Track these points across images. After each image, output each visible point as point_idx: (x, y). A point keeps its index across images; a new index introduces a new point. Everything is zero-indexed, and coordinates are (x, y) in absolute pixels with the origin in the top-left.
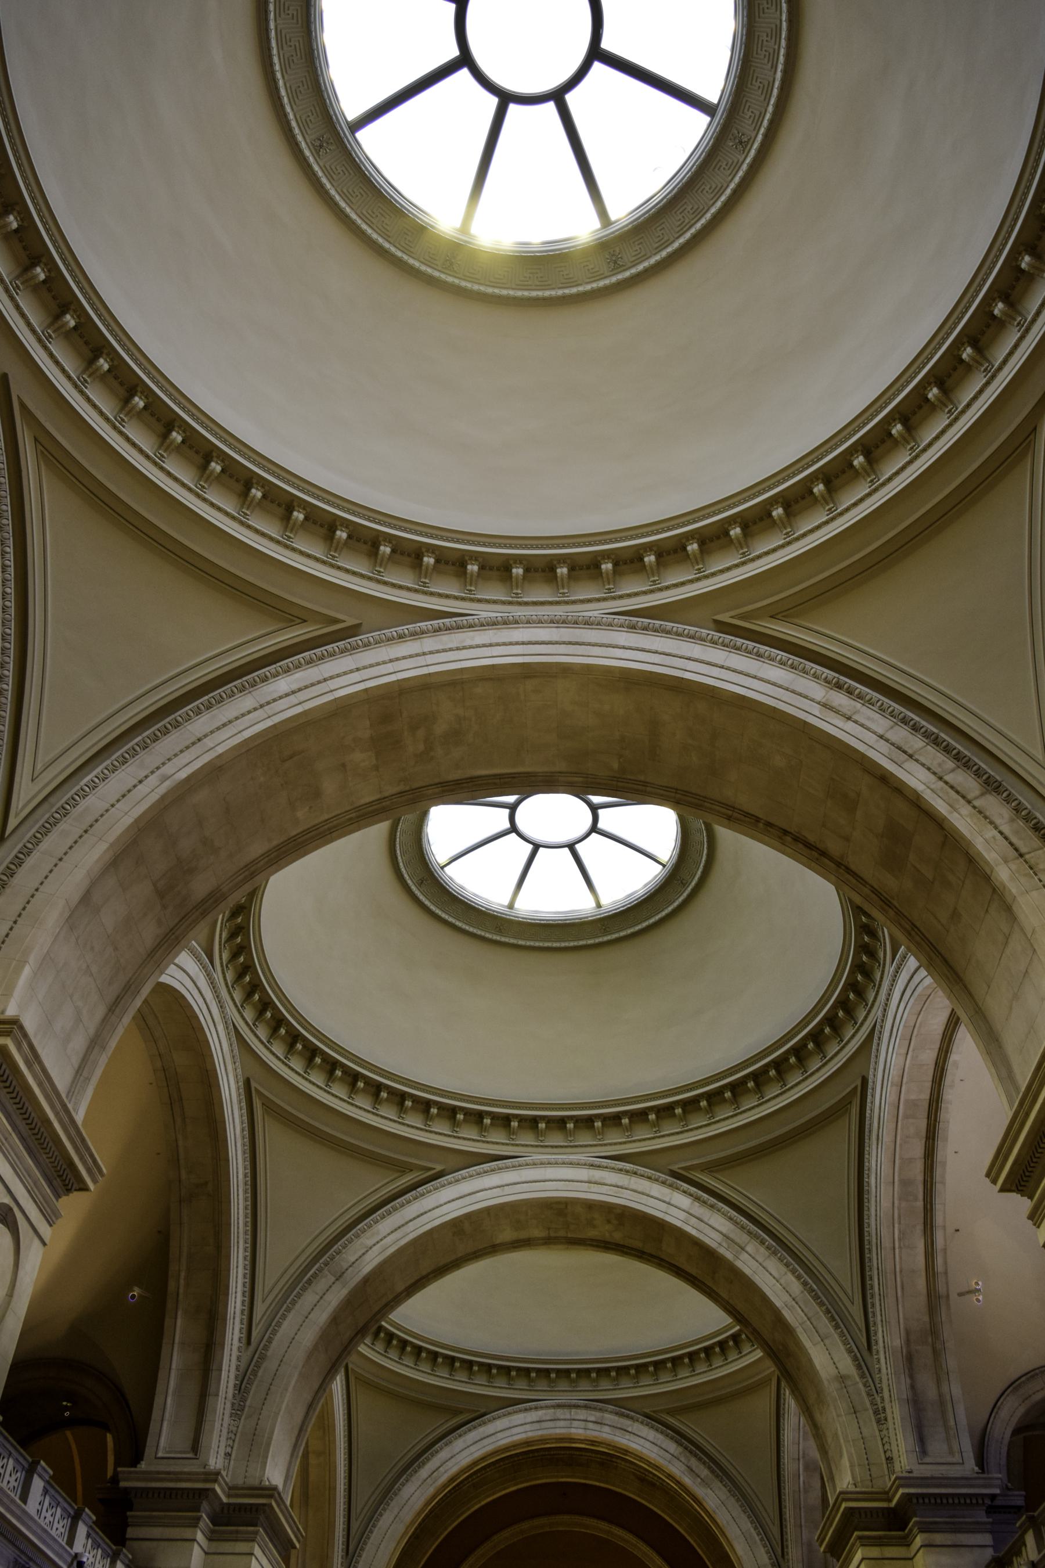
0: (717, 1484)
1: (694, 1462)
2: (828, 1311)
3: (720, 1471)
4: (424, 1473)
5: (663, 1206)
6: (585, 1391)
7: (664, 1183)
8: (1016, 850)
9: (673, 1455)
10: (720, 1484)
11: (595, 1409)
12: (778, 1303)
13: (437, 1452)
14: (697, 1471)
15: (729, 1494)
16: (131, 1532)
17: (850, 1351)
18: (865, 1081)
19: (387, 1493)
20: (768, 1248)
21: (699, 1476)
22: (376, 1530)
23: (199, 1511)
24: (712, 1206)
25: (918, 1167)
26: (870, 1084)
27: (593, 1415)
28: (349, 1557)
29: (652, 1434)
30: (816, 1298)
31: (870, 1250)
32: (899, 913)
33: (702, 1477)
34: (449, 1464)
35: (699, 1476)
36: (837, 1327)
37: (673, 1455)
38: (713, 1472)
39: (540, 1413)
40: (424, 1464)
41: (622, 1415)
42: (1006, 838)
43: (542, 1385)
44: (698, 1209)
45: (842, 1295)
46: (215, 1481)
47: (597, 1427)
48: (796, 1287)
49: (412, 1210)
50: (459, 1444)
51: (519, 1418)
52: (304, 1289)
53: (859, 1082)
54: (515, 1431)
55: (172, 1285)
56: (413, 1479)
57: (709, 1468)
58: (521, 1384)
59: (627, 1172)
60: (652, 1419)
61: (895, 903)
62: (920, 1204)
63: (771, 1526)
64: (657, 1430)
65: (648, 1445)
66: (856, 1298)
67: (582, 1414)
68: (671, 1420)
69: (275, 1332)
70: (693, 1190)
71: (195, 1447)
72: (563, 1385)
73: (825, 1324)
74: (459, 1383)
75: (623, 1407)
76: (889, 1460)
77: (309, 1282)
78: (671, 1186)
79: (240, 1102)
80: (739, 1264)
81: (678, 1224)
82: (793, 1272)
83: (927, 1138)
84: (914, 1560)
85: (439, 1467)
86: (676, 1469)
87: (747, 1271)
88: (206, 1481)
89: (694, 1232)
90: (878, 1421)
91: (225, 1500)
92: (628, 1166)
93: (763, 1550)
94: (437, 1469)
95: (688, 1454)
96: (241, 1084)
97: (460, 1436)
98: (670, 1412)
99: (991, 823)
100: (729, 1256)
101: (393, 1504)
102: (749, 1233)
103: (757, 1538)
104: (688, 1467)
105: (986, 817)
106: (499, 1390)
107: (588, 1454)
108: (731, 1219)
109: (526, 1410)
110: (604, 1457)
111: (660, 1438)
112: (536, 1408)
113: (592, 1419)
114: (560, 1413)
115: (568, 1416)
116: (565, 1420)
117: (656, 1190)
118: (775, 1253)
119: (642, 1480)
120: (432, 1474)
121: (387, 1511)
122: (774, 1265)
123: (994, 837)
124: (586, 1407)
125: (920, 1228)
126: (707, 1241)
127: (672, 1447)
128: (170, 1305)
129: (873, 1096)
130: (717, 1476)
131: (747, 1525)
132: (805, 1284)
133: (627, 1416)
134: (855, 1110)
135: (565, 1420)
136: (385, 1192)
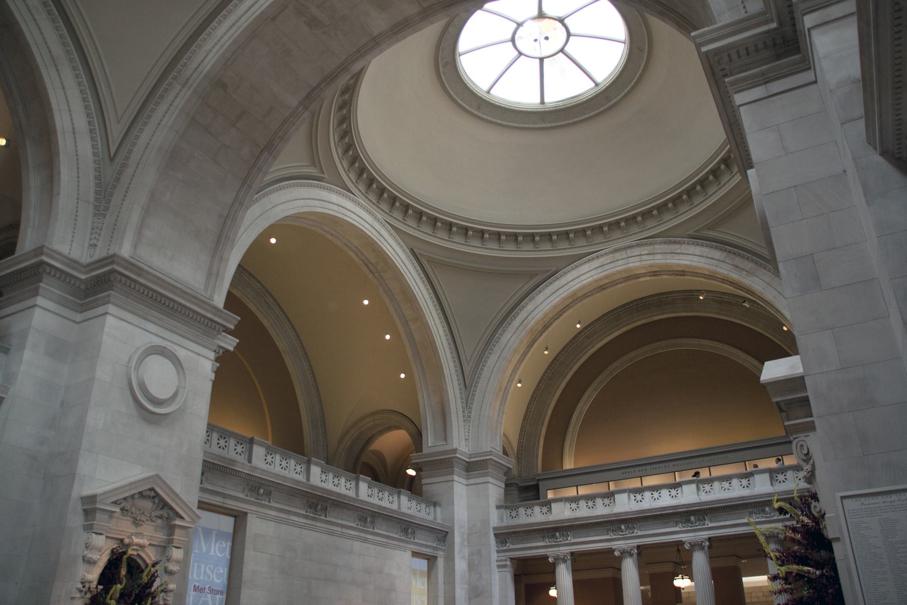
1: (738, 261)
4: (516, 323)
9: (719, 260)
10: (765, 272)
11: (646, 244)
13: (524, 307)
14: (742, 267)
19: (489, 342)
21: (744, 270)
22: (486, 369)
27: (645, 250)
29: (698, 250)
34: (535, 313)
35: (744, 270)
37: (719, 260)
39: (602, 260)
40: (515, 317)
41: (671, 243)
46: (42, 254)
47: (651, 257)
50: (540, 298)
51: (586, 268)
54: (582, 278)
57: (752, 261)
58: (582, 242)
60: (697, 238)
64: (702, 245)
65: (696, 258)
67: (636, 251)
72: (617, 234)
74: (527, 252)
75: (669, 237)
85: (527, 317)
86: (724, 270)
88: (36, 256)
91: (83, 277)
94: (526, 319)
95: (732, 256)
97: (540, 292)
98: (710, 227)
106: (564, 250)
109: (589, 260)
110: (686, 294)
111: (706, 251)
112: (598, 257)
113: (646, 252)
114: (617, 256)
115: (625, 256)
116: (623, 259)
120: (522, 323)
124: (638, 245)
127: (718, 254)
130: (761, 265)
133: (675, 242)
135: (623, 259)
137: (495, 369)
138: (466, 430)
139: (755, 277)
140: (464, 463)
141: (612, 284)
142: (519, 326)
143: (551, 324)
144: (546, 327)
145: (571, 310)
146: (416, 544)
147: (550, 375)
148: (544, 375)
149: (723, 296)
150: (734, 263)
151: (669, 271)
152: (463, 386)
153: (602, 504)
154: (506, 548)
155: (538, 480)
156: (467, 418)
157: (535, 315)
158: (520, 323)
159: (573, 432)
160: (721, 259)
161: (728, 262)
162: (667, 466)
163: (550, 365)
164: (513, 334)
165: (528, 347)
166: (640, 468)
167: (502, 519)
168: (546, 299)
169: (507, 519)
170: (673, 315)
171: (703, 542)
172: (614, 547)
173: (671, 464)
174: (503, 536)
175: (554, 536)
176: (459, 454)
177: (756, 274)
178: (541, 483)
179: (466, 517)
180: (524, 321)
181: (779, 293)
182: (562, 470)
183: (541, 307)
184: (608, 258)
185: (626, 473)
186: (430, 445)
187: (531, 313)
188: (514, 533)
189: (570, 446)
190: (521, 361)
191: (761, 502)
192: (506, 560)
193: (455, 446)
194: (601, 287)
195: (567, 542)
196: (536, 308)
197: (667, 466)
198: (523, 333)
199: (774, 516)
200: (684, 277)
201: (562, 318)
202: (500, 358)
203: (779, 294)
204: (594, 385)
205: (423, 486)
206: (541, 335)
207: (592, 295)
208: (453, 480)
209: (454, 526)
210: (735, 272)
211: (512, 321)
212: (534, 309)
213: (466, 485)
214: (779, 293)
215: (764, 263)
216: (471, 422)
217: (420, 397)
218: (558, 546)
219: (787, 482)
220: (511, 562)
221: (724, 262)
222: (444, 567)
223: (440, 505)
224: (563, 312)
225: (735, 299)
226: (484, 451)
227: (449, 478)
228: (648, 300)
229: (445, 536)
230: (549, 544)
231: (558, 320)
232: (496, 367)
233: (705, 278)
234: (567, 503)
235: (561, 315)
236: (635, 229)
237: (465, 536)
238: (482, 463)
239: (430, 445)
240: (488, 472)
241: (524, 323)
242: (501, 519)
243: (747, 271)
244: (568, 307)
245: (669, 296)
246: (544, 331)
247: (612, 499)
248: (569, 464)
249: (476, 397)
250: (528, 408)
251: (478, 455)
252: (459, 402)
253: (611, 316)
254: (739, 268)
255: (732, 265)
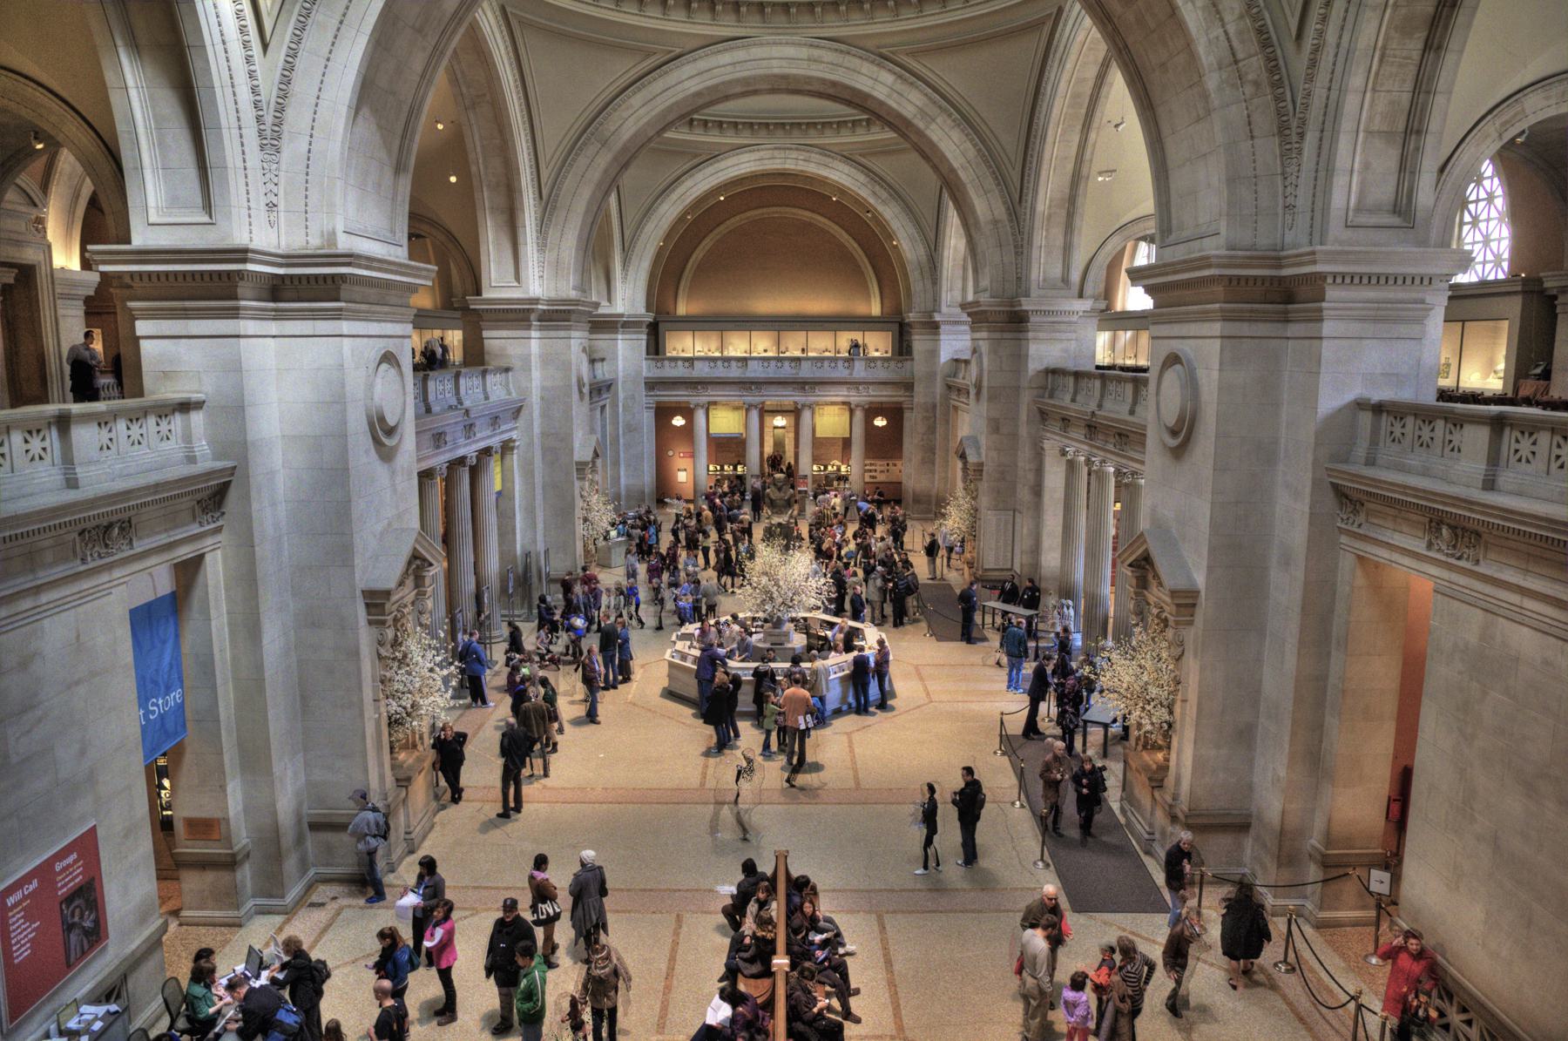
1: (877, 188)
2: (994, 172)
3: (896, 194)
4: (674, 196)
5: (870, 83)
6: (797, 138)
7: (873, 62)
8: (1234, 55)
12: (956, 165)
17: (1005, 203)
18: (1060, 10)
19: (648, 211)
20: (954, 121)
24: (911, 84)
25: (1091, 84)
26: (1064, 15)
27: (803, 155)
29: (846, 169)
30: (986, 162)
31: (1035, 137)
32: (1115, 29)
34: (694, 189)
36: (999, 184)
39: (762, 153)
42: (1229, 39)
43: (763, 133)
44: (899, 86)
45: (1006, 161)
48: (972, 153)
49: (658, 86)
50: (699, 176)
51: (745, 157)
52: (577, 155)
53: (1055, 10)
55: (474, 169)
58: (747, 133)
59: (842, 52)
60: (848, 159)
61: (1115, 20)
62: (1083, 111)
67: (794, 154)
68: (863, 160)
69: (560, 189)
70: (897, 69)
71: (518, 278)
72: (780, 133)
73: (990, 182)
75: (824, 150)
76: (1019, 279)
77: (581, 149)
78: (878, 65)
79: (500, 27)
80: (928, 132)
81: (882, 97)
82: (971, 141)
83: (1102, 65)
86: (864, 193)
87: (935, 138)
89: (894, 105)
90: (1016, 253)
92: (843, 47)
96: (498, 13)
99: (1222, 20)
100: (921, 125)
102: (940, 107)
105: (1218, 12)
106: (730, 139)
108: (926, 95)
114: (776, 153)
117: (867, 68)
118: (959, 125)
122: (956, 135)
123: (1217, 38)
124: (797, 149)
125: (1079, 127)
126: (905, 113)
127: (862, 178)
128: (476, 183)
129: (1065, 25)
131: (911, 230)
132: (979, 150)
134: (1047, 28)
136: (633, 74)
174: (652, 385)
178: (661, 325)
184: (767, 154)
236: (796, 132)
242: (649, 370)
248: (682, 309)
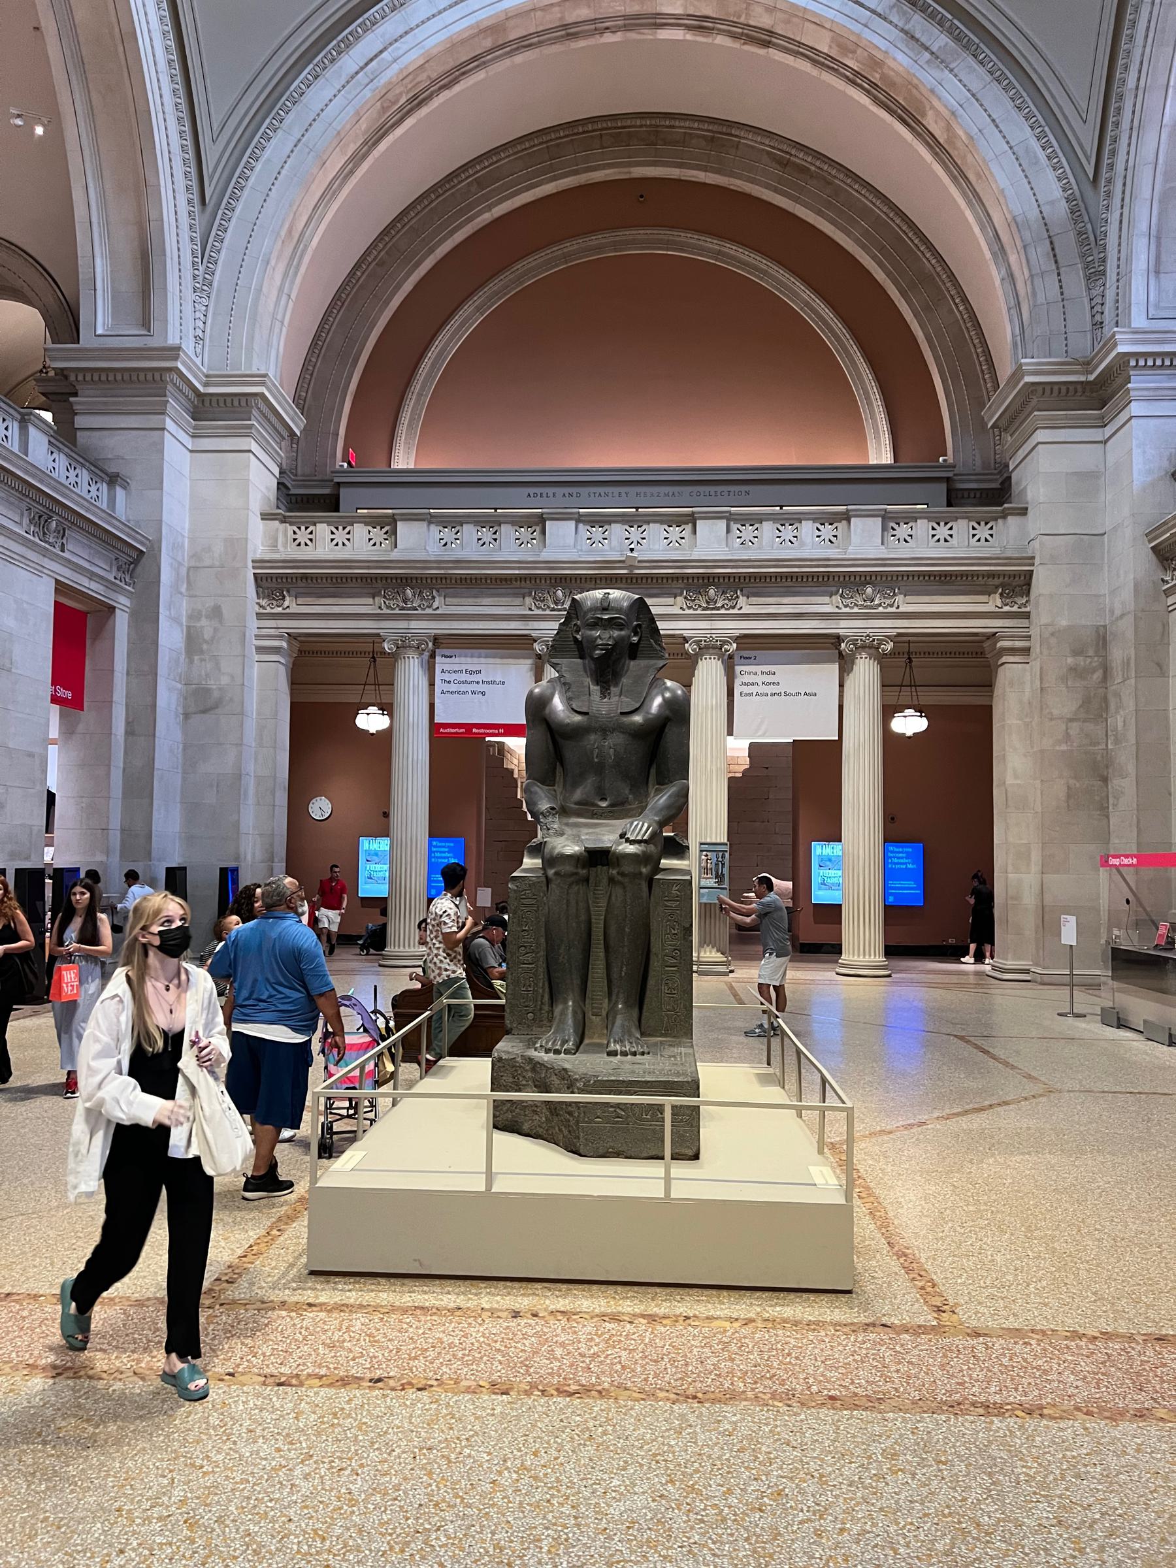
0: (965, 63)
4: (350, 61)
9: (873, 12)
14: (923, 39)
15: (988, 78)
16: (80, 421)
21: (927, 49)
23: (165, 396)
28: (209, 208)
33: (934, 50)
35: (927, 49)
37: (873, 12)
38: (958, 39)
56: (328, 74)
57: (951, 31)
63: (1076, 123)
66: (1091, 117)
84: (1109, 444)
85: (381, 52)
93: (1051, 175)
94: (376, 56)
101: (289, 119)
103: (1042, 155)
104: (906, 33)
107: (687, 124)
110: (715, 128)
119: (784, 164)
120: (367, 64)
121: (280, 132)
137: (283, 172)
138: (198, 315)
139: (947, 72)
140: (191, 395)
141: (593, 27)
142: (357, 73)
143: (430, 98)
144: (417, 101)
145: (481, 75)
146: (68, 563)
147: (382, 254)
148: (367, 252)
149: (793, 152)
150: (906, 28)
151: (735, 24)
152: (196, 201)
153: (513, 540)
154: (280, 610)
155: (339, 484)
156: (203, 286)
157: (401, 52)
158: (361, 64)
159: (420, 395)
160: (879, 10)
161: (895, 20)
162: (623, 495)
163: (385, 232)
164: (339, 91)
165: (365, 143)
166: (567, 490)
167: (274, 547)
168: (434, 16)
169: (285, 545)
170: (674, 173)
171: (724, 642)
172: (534, 634)
173: (633, 490)
175: (400, 593)
176: (184, 363)
177: (952, 66)
178: (343, 492)
179: (187, 526)
180: (372, 60)
181: (993, 121)
182: (388, 469)
183: (420, 34)
185: (535, 495)
186: (99, 332)
187: (391, 44)
188: (305, 577)
189: (410, 425)
190: (357, 159)
191: (860, 574)
192: (280, 637)
193: (172, 340)
194: (565, 26)
195: (429, 611)
196: (406, 33)
197: (623, 495)
198: (367, 93)
199: (880, 605)
200: (762, 51)
201: (457, 88)
202: (300, 145)
203: (992, 125)
204: (477, 299)
205: (79, 434)
206: (401, 121)
207: (540, 44)
208: (163, 429)
209: (160, 541)
210: (906, 50)
211: (339, 53)
212: (401, 37)
213: (191, 451)
214: (993, 121)
215: (976, 40)
216: (213, 296)
217: (77, 195)
218: (408, 618)
219: (912, 542)
220: (289, 643)
221: (885, 19)
222: (128, 634)
223: (125, 486)
224: (464, 73)
225: (818, 163)
226: (243, 371)
227: (153, 421)
228: (629, 123)
229: (136, 562)
230: (385, 611)
231: (447, 92)
232: (287, 166)
233: (814, 62)
234: (433, 527)
235: (455, 81)
237: (184, 571)
238: (236, 403)
239: (99, 332)
240: (251, 427)
241: (370, 66)
243: (933, 53)
244: (477, 61)
245: (677, 123)
246: (409, 113)
247: (538, 529)
248: (404, 459)
249: (228, 237)
250: (324, 320)
251: (228, 380)
252: (185, 234)
253: (541, 144)
254: (917, 40)
255: (902, 30)
